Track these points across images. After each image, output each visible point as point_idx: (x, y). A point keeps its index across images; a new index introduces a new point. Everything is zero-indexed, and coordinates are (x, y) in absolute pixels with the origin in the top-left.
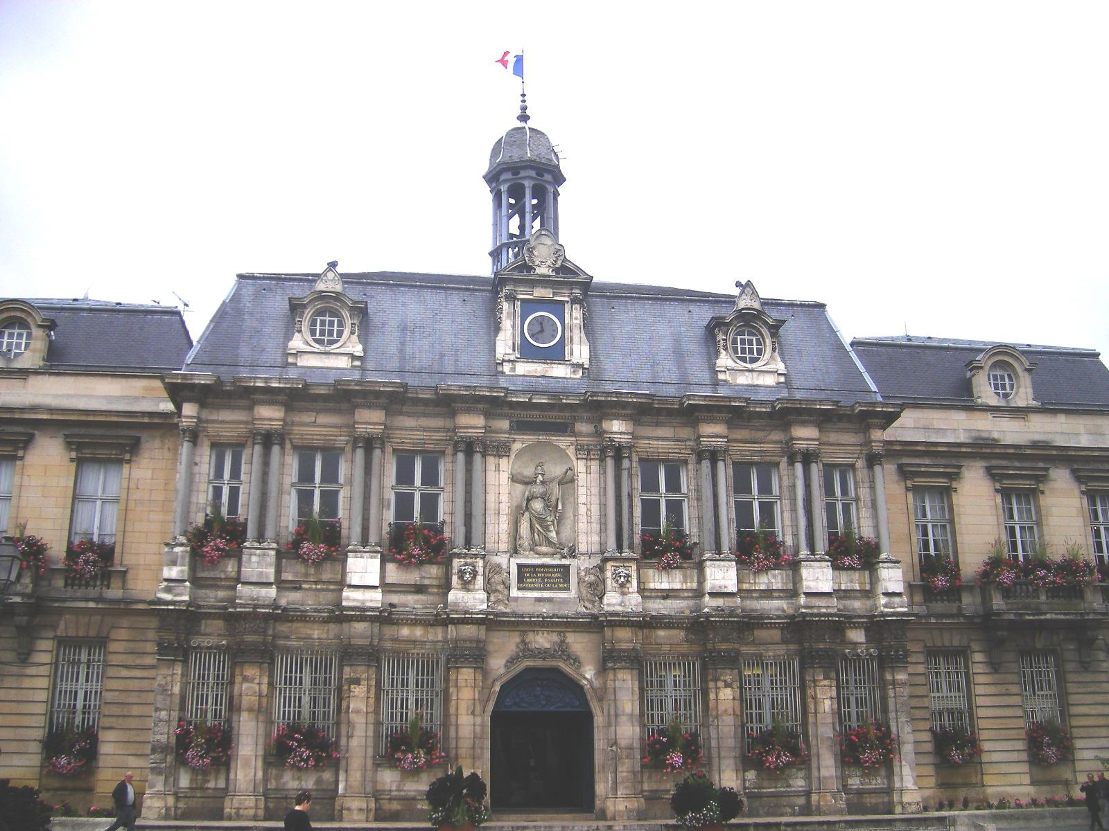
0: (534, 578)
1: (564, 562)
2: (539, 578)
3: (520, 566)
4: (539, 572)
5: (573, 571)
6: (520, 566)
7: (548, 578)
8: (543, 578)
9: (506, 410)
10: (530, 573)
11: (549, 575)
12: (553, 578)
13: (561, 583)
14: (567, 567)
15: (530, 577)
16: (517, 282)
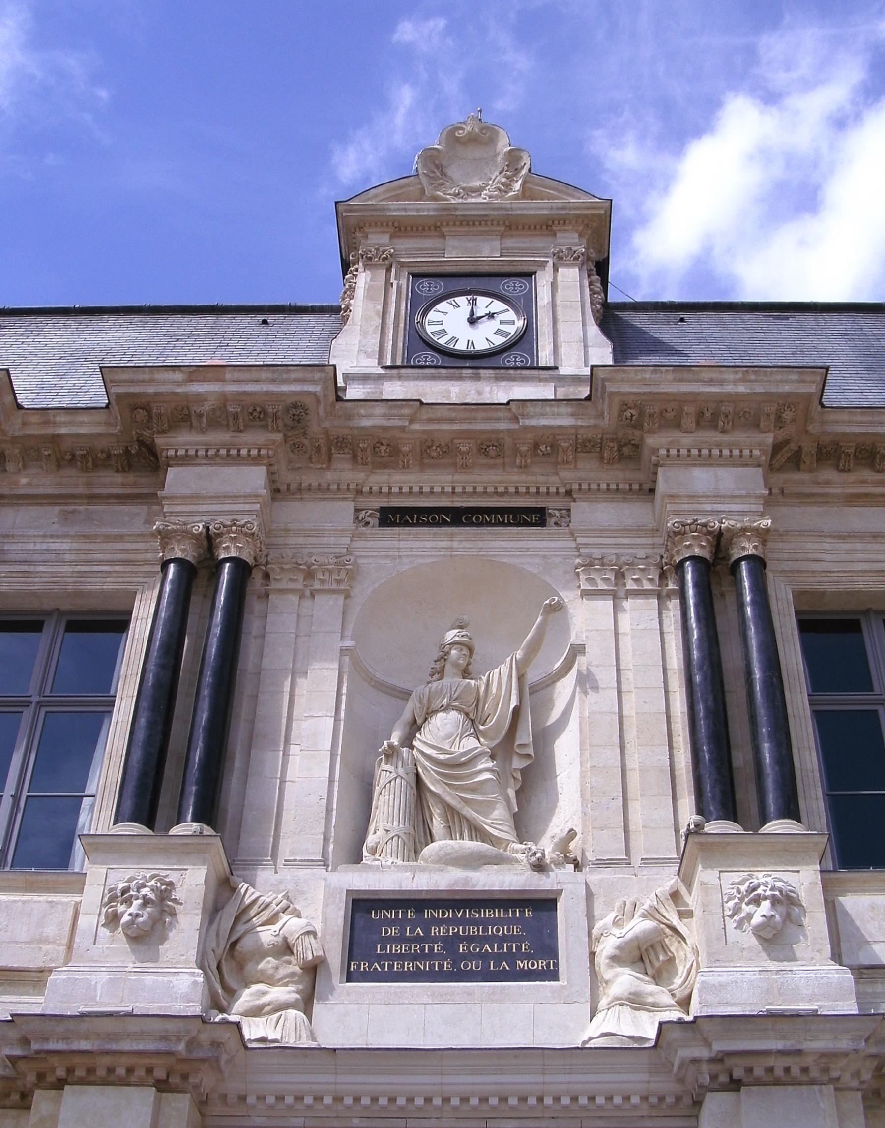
0: (417, 939)
1: (543, 883)
2: (435, 940)
3: (362, 906)
4: (439, 922)
5: (568, 916)
6: (362, 906)
7: (470, 939)
8: (450, 943)
9: (344, 473)
10: (401, 924)
11: (472, 930)
12: (490, 940)
13: (528, 957)
14: (544, 905)
15: (401, 939)
16: (401, 228)
